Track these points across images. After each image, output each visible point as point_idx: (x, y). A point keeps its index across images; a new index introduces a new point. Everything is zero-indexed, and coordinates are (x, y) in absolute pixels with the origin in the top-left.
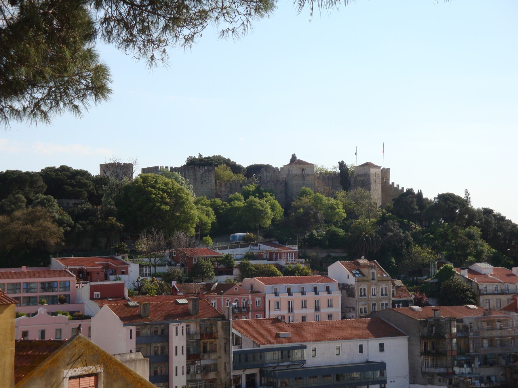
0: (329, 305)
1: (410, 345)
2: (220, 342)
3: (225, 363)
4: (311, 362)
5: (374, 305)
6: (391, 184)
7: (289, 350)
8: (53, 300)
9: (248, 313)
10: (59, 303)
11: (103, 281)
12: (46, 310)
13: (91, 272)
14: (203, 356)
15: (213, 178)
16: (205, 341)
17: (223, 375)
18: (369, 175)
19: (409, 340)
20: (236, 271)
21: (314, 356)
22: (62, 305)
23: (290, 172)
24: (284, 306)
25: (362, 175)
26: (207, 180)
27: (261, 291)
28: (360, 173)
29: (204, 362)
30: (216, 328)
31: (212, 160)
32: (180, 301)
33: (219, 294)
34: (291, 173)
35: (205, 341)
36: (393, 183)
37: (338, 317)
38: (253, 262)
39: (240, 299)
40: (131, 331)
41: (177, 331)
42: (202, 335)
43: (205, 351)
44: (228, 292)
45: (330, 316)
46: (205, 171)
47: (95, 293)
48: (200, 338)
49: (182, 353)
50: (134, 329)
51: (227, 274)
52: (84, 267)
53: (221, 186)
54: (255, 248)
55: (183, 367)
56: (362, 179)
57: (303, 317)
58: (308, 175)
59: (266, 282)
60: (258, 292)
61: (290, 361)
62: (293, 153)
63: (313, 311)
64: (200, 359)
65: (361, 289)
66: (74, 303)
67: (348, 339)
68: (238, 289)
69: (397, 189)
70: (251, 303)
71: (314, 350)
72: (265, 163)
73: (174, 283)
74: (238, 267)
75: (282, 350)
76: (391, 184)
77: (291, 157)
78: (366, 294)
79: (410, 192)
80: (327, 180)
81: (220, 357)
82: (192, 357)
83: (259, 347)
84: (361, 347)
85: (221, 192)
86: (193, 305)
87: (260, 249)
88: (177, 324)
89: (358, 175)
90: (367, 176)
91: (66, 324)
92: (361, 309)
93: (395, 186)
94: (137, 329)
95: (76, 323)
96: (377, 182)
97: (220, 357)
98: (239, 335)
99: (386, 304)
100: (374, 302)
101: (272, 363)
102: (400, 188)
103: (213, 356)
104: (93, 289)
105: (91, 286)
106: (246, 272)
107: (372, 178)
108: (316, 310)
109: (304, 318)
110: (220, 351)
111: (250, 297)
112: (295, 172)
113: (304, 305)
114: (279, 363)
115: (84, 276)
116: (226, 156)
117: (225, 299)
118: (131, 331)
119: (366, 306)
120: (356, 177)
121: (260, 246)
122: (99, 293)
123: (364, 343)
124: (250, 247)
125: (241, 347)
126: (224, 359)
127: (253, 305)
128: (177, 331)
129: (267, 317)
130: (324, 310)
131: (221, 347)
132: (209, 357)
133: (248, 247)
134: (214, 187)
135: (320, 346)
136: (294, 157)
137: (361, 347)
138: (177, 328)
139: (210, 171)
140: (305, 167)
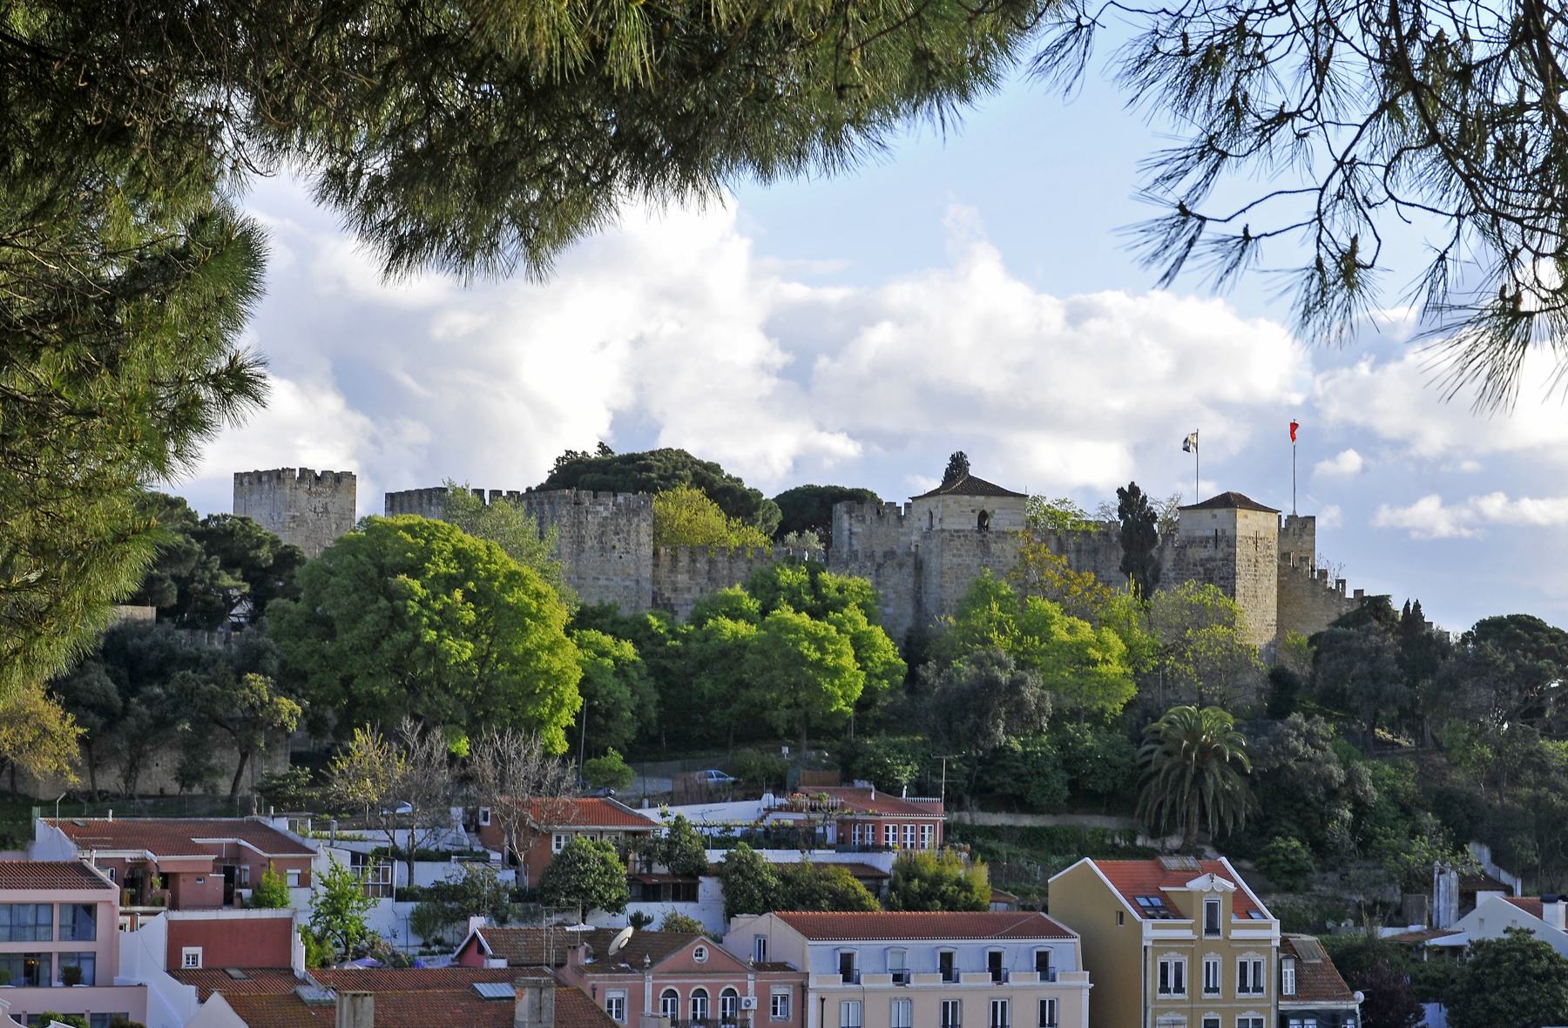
12: (7, 1005)
18: (1231, 542)
20: (708, 887)
23: (936, 521)
25: (1208, 538)
27: (793, 962)
28: (1199, 533)
32: (486, 990)
33: (638, 966)
34: (937, 526)
36: (1323, 574)
44: (671, 960)
46: (616, 515)
47: (187, 950)
51: (676, 898)
52: (150, 855)
53: (674, 567)
59: (811, 931)
60: (782, 967)
62: (954, 452)
65: (1164, 966)
68: (706, 953)
70: (754, 1005)
74: (718, 871)
78: (1185, 984)
79: (1377, 606)
85: (675, 590)
86: (532, 1004)
89: (1191, 542)
90: (1223, 545)
96: (1261, 566)
104: (178, 936)
111: (751, 985)
112: (951, 524)
117: (656, 988)
122: (198, 950)
134: (647, 572)
136: (958, 464)
139: (636, 512)
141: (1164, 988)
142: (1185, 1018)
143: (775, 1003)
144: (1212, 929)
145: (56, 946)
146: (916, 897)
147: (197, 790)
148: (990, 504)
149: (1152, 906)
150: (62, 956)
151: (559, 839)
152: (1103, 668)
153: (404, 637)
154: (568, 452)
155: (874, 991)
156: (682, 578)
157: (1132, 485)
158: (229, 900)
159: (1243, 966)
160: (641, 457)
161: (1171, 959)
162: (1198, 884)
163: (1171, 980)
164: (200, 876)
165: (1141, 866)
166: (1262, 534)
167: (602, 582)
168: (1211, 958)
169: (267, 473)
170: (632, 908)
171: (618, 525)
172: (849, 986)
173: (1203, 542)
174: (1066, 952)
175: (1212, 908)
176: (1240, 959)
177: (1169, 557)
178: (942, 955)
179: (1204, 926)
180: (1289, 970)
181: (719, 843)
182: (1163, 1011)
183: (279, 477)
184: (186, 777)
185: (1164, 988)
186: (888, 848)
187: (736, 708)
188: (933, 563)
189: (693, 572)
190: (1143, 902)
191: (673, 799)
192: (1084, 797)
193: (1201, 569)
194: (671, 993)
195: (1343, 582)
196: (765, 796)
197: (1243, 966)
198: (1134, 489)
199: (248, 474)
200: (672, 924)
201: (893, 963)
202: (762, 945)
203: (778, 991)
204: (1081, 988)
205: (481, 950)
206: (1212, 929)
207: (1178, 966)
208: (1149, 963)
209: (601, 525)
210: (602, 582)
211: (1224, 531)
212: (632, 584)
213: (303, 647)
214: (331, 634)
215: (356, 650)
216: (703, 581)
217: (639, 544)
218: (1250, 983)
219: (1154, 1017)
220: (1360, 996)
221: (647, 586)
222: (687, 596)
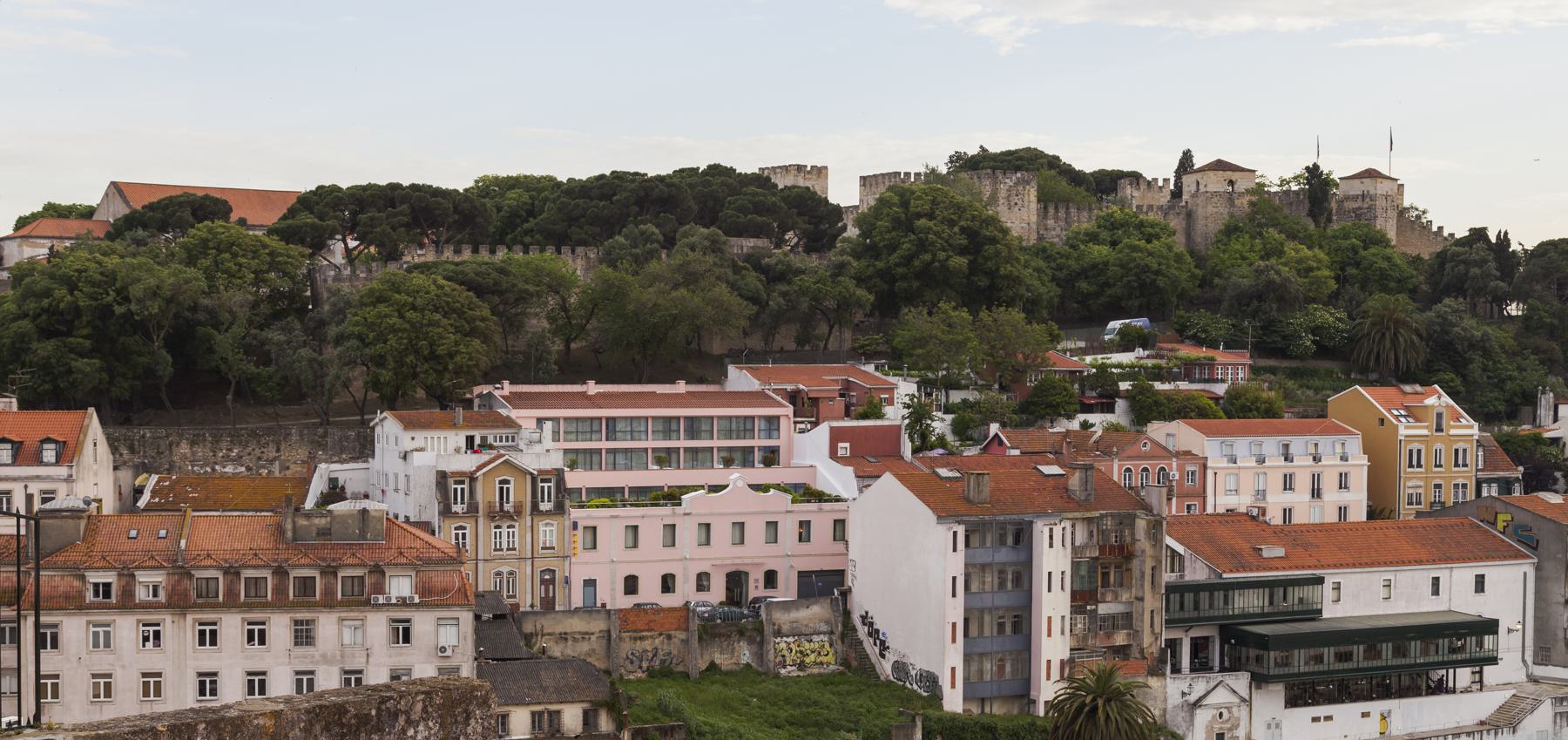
0: (1343, 484)
1: (1539, 579)
4: (1332, 611)
5: (1438, 486)
8: (741, 458)
15: (1033, 198)
17: (1147, 640)
19: (1538, 568)
20: (1120, 404)
29: (1103, 609)
30: (1133, 534)
31: (1021, 158)
37: (1358, 514)
38: (1158, 386)
39: (1154, 466)
40: (955, 533)
41: (1051, 537)
42: (1102, 549)
44: (1130, 451)
46: (1016, 184)
47: (841, 445)
50: (961, 530)
56: (1355, 205)
59: (1209, 433)
60: (1188, 453)
63: (1308, 497)
65: (1411, 452)
67: (1410, 563)
71: (1337, 587)
72: (1126, 168)
73: (994, 428)
74: (1127, 395)
82: (1082, 599)
84: (1436, 581)
89: (1347, 198)
95: (808, 510)
98: (1180, 549)
99: (1464, 486)
100: (1438, 481)
104: (836, 436)
105: (832, 429)
106: (1147, 409)
107: (1380, 203)
109: (1287, 513)
112: (1212, 188)
113: (1288, 484)
115: (807, 408)
116: (1050, 151)
117: (1120, 467)
118: (955, 533)
122: (847, 445)
123: (1443, 573)
127: (1180, 482)
128: (1051, 537)
129: (1210, 510)
130: (1332, 496)
131: (1143, 575)
134: (1034, 219)
135: (1352, 580)
137: (1436, 581)
141: (1411, 466)
144: (1439, 429)
145: (758, 442)
146: (1240, 410)
147: (807, 348)
148: (1235, 176)
152: (1319, 273)
153: (927, 257)
156: (1051, 222)
158: (848, 414)
160: (1016, 151)
161: (1415, 446)
162: (1431, 401)
163: (1415, 460)
168: (1438, 446)
170: (1081, 417)
174: (1354, 445)
175: (1439, 416)
177: (1334, 205)
180: (1480, 453)
181: (1123, 377)
184: (800, 342)
185: (1411, 466)
186: (1217, 381)
187: (1103, 299)
188: (1200, 211)
189: (1056, 219)
191: (1085, 352)
192: (1323, 351)
194: (1128, 470)
198: (1316, 167)
200: (1113, 429)
201: (1255, 450)
203: (1190, 468)
205: (1001, 443)
206: (1439, 429)
207: (1419, 451)
213: (864, 262)
214: (877, 257)
215: (897, 265)
216: (1062, 224)
220: (1521, 469)
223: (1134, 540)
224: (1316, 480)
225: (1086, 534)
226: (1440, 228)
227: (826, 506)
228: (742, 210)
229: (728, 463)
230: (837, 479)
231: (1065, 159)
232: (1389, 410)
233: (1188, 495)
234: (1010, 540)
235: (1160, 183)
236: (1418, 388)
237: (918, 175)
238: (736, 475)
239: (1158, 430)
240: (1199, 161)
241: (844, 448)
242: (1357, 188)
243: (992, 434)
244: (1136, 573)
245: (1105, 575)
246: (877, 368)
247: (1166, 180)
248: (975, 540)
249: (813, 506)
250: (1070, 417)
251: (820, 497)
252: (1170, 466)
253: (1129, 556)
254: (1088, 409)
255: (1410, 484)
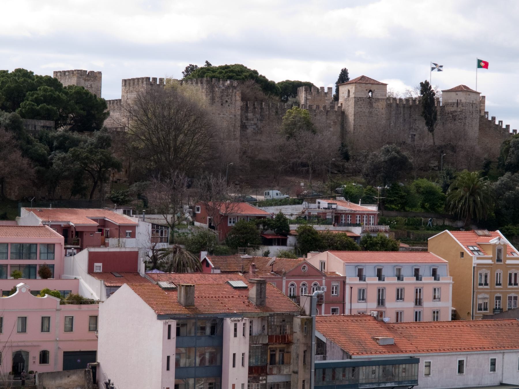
2: (297, 349)
3: (304, 381)
5: (498, 298)
6: (490, 119)
7: (395, 363)
8: (29, 272)
9: (321, 305)
10: (38, 277)
11: (99, 246)
13: (82, 232)
14: (271, 369)
15: (238, 98)
16: (274, 346)
20: (291, 240)
21: (428, 375)
22: (45, 281)
24: (372, 295)
25: (454, 103)
26: (229, 101)
28: (450, 101)
30: (292, 328)
31: (232, 71)
35: (274, 346)
36: (494, 118)
40: (169, 326)
41: (235, 330)
42: (270, 338)
43: (273, 362)
45: (436, 313)
47: (96, 264)
48: (267, 342)
49: (243, 365)
50: (174, 324)
54: (313, 206)
55: (243, 385)
56: (453, 109)
57: (397, 313)
58: (378, 100)
61: (395, 382)
62: (343, 68)
63: (412, 304)
64: (267, 374)
66: (60, 278)
68: (306, 268)
69: (499, 127)
71: (428, 365)
72: (303, 79)
73: (204, 255)
75: (384, 363)
76: (490, 119)
77: (339, 72)
78: (488, 282)
80: (402, 109)
81: (296, 373)
83: (351, 358)
84: (493, 363)
86: (257, 290)
87: (319, 207)
88: (236, 319)
89: (446, 104)
90: (460, 106)
91: (57, 310)
92: (480, 305)
93: (497, 123)
94: (177, 324)
95: (72, 309)
96: (474, 114)
97: (296, 373)
100: (498, 295)
101: (369, 383)
102: (504, 127)
103: (286, 370)
104: (93, 258)
105: (90, 253)
108: (416, 304)
110: (297, 363)
111: (324, 281)
113: (400, 296)
114: (379, 383)
115: (74, 237)
117: (287, 283)
118: (169, 326)
119: (486, 301)
120: (443, 107)
121: (319, 203)
122: (100, 264)
124: (305, 204)
125: (325, 358)
126: (302, 375)
128: (235, 330)
132: (280, 370)
133: (301, 204)
134: (239, 112)
138: (236, 325)
140: (373, 88)
142: (487, 296)
143: (333, 289)
144: (499, 260)
149: (475, 250)
150: (12, 266)
151: (230, 219)
154: (190, 65)
155: (371, 284)
157: (426, 81)
159: (510, 274)
162: (494, 241)
164: (92, 233)
165: (468, 235)
166: (474, 102)
167: (221, 116)
168: (499, 271)
169: (68, 71)
171: (228, 92)
172: (381, 282)
173: (452, 104)
176: (509, 272)
178: (415, 269)
179: (496, 258)
182: (480, 293)
183: (73, 73)
189: (254, 112)
190: (471, 248)
193: (451, 116)
195: (502, 122)
196: (304, 203)
197: (510, 274)
199: (60, 72)
202: (323, 264)
204: (449, 283)
205: (208, 265)
206: (499, 260)
208: (475, 273)
209: (222, 92)
210: (221, 116)
211: (461, 100)
212: (233, 116)
216: (258, 116)
217: (236, 101)
218: (513, 282)
219: (477, 296)
221: (239, 117)
222: (252, 122)
223: (292, 333)
224: (418, 292)
225: (260, 328)
226: (508, 126)
227: (84, 307)
228: (38, 101)
229: (16, 276)
230: (91, 288)
231: (261, 73)
232: (467, 247)
233: (333, 303)
234: (208, 331)
235: (326, 90)
236: (486, 232)
237: (161, 80)
238: (21, 284)
239: (315, 259)
240: (352, 76)
241: (98, 266)
242: (453, 98)
243: (202, 259)
244: (293, 355)
245: (273, 356)
246: (125, 212)
247: (330, 89)
248: (183, 330)
249: (75, 307)
250: (256, 247)
251: (79, 301)
252: (321, 282)
253: (289, 343)
254: (269, 242)
255: (480, 296)
